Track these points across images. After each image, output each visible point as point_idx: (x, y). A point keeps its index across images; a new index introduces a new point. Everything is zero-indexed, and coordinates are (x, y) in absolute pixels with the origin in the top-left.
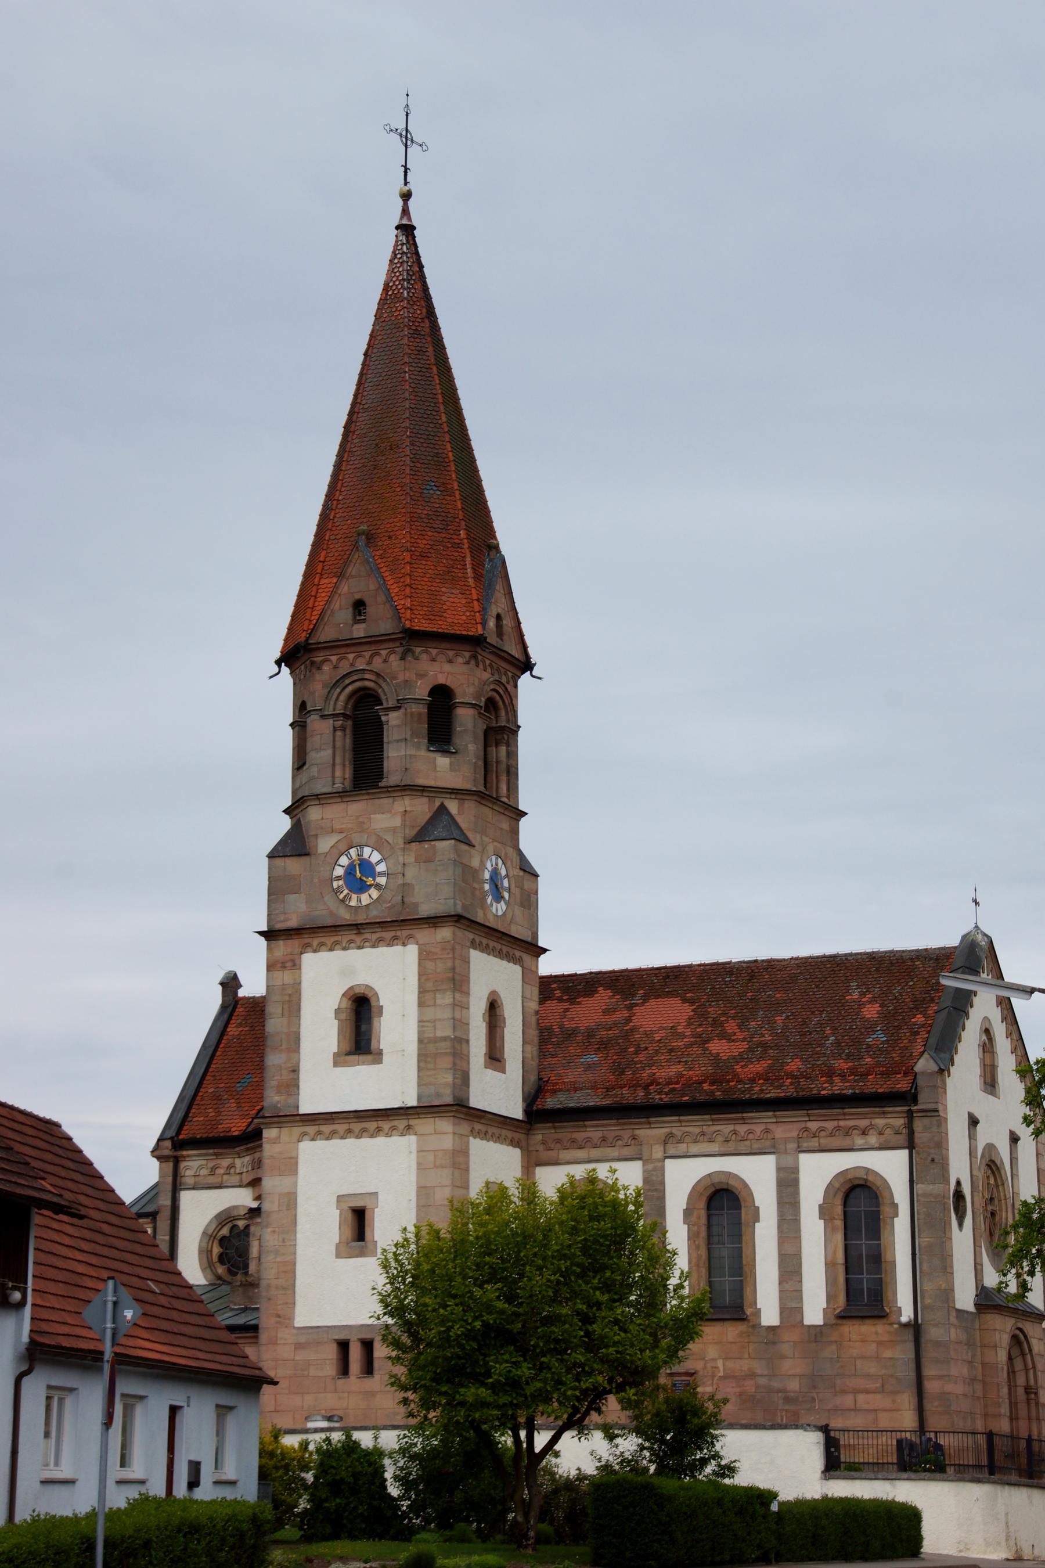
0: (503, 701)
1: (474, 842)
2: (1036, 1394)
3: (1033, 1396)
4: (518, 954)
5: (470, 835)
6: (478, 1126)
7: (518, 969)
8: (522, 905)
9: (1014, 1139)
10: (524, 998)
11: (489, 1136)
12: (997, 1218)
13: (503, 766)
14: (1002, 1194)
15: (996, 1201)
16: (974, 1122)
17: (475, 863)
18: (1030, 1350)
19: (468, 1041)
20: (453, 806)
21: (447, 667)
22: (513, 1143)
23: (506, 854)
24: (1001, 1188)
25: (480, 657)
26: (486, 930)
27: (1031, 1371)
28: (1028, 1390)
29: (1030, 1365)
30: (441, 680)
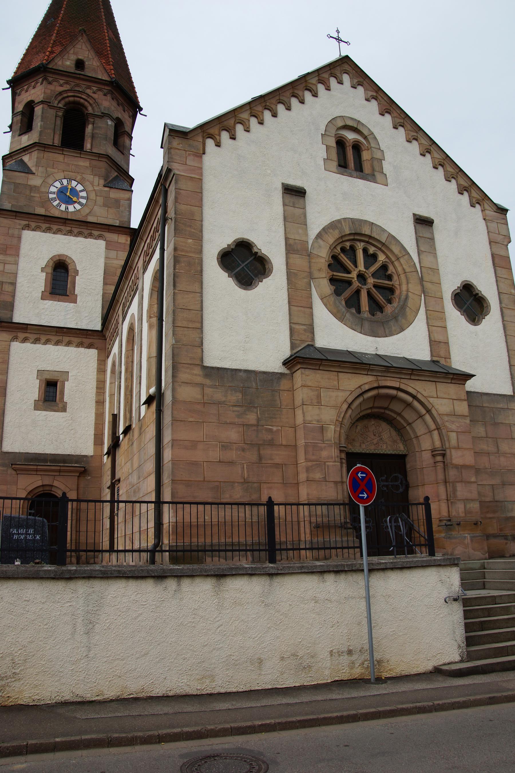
0: (88, 102)
1: (34, 171)
2: (444, 455)
3: (439, 458)
4: (96, 233)
5: (33, 169)
6: (21, 335)
7: (102, 243)
8: (105, 205)
9: (423, 222)
10: (106, 258)
11: (43, 341)
12: (397, 292)
13: (90, 135)
14: (400, 269)
15: (395, 278)
16: (294, 193)
17: (35, 181)
18: (429, 411)
19: (14, 284)
20: (26, 159)
21: (33, 91)
22: (90, 346)
23: (83, 178)
24: (396, 263)
25: (50, 79)
26: (43, 218)
27: (436, 433)
28: (434, 453)
29: (433, 426)
30: (29, 99)
